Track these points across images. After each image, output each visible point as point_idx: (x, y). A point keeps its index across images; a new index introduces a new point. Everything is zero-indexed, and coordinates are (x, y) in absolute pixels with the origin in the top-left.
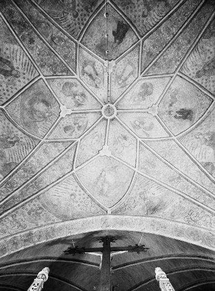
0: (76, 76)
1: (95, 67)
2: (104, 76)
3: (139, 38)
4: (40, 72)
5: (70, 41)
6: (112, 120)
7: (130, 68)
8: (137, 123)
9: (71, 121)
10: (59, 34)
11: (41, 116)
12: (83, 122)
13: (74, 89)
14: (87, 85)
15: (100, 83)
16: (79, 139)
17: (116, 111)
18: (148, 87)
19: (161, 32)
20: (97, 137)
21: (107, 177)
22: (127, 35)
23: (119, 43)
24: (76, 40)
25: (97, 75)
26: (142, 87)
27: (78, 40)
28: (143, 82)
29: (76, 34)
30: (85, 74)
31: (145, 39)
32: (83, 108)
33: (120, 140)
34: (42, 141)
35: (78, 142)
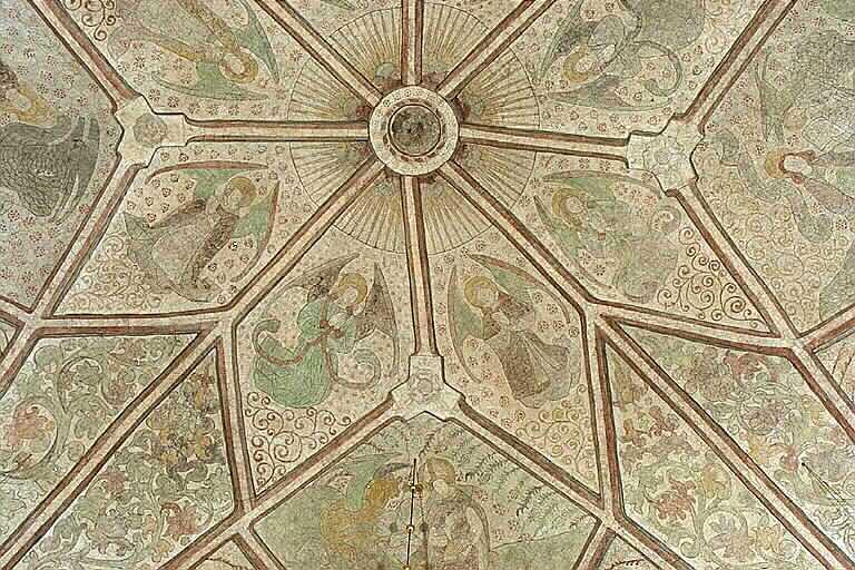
0: (223, 331)
2: (206, 165)
4: (220, 539)
5: (27, 370)
11: (448, 520)
12: (475, 283)
13: (289, 336)
15: (248, 190)
16: (590, 310)
17: (413, 91)
20: (570, 201)
21: (823, 143)
24: (23, 340)
27: (19, 326)
30: (205, 273)
32: (397, 283)
33: (586, 63)
34: (615, 527)
35: (610, 320)
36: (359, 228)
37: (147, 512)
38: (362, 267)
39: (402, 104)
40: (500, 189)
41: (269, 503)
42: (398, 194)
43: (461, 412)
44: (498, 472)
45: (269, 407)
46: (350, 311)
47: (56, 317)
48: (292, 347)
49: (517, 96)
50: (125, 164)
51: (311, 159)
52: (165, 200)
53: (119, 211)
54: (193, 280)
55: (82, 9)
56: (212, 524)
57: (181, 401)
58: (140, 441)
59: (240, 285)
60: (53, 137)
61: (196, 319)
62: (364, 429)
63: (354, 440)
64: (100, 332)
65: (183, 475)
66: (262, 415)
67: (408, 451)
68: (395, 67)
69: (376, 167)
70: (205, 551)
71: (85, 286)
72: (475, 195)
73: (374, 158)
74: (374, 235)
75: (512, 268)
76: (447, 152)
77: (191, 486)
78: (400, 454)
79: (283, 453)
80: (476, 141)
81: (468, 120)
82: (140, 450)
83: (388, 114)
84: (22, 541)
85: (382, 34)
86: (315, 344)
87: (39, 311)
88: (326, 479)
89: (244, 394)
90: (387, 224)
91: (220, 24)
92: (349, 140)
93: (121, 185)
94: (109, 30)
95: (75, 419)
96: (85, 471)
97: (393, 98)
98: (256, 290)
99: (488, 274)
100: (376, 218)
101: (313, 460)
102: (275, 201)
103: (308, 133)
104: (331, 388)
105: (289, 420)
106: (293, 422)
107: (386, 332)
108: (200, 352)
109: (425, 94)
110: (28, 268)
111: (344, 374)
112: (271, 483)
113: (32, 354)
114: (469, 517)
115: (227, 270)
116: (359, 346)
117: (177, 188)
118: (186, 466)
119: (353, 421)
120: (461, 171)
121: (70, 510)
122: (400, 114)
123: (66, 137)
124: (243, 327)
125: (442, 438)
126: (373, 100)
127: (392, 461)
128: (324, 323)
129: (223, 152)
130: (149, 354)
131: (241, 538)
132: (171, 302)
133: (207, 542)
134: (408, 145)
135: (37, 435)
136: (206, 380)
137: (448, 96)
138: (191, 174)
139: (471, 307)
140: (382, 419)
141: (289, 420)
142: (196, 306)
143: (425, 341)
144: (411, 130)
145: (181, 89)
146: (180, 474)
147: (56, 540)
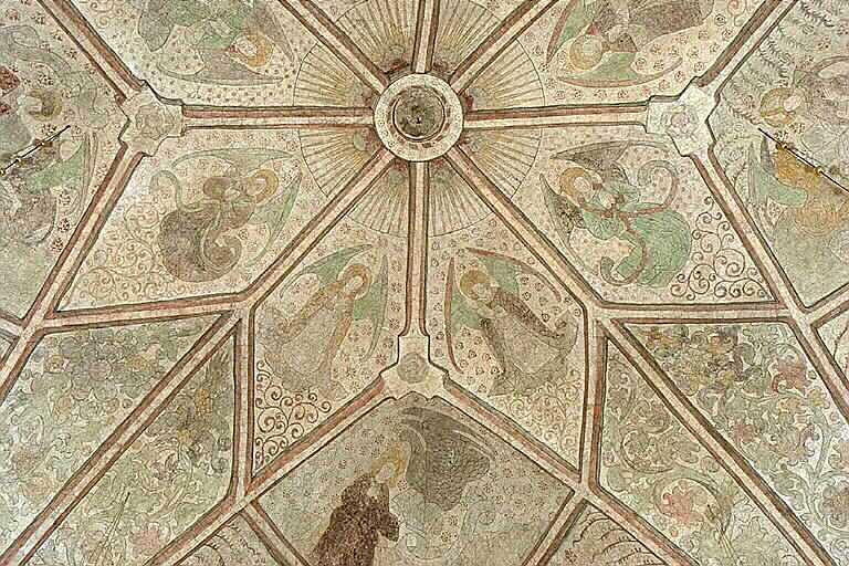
0: (606, 316)
1: (494, 362)
2: (448, 314)
3: (251, 511)
5: (628, 499)
6: (402, 66)
7: (298, 357)
8: (246, 47)
9: (651, 59)
10: (684, 531)
12: (575, 56)
13: (617, 249)
14: (540, 268)
15: (473, 277)
18: (193, 258)
19: (135, 538)
22: (322, 522)
23: (364, 481)
25: (485, 323)
26: (226, 258)
27: (585, 503)
28: (221, 286)
29: (595, 531)
30: (551, 325)
31: (219, 509)
32: (576, 138)
36: (515, 173)
37: (779, 406)
38: (554, 171)
39: (393, 128)
40: (479, 30)
41: (783, 291)
42: (483, 133)
43: (709, 86)
44: (780, 46)
45: (687, 277)
46: (596, 186)
47: (580, 470)
48: (630, 248)
49: (385, 13)
50: (442, 392)
51: (446, 217)
52: (479, 356)
53: (486, 400)
54: (557, 337)
55: (302, 422)
56: (800, 348)
57: (672, 361)
58: (708, 404)
59: (564, 294)
60: (420, 445)
61: (593, 342)
62: (718, 187)
63: (728, 198)
64: (598, 429)
65: (746, 366)
66: (694, 283)
67: (747, 138)
68: (356, 133)
69: (454, 156)
70: (824, 360)
71: (553, 440)
72: (484, 59)
73: (445, 157)
74: (523, 158)
75: (563, 18)
76: (441, 86)
77: (758, 360)
78: (752, 145)
79: (735, 268)
80: (430, 53)
81: (408, 60)
82: (716, 404)
83: (402, 142)
84: (788, 528)
85: (325, 146)
86: (628, 224)
87: (574, 485)
88: (766, 227)
89: (671, 299)
90: (512, 145)
91: (318, 297)
92: (427, 180)
93: (461, 398)
94: (321, 399)
95: (681, 462)
96: (729, 461)
97: (387, 138)
98: (569, 282)
99: (568, 45)
100: (505, 155)
101: (744, 240)
102: (485, 253)
103: (419, 220)
104: (675, 212)
105: (702, 258)
106: (705, 254)
107: (621, 152)
108: (625, 341)
109: (382, 107)
110: (536, 486)
111: (660, 199)
112: (764, 285)
113: (615, 494)
114: (827, 76)
115: (548, 305)
116: (633, 181)
117: (468, 344)
118: (737, 363)
119: (709, 194)
120: (460, 71)
121: (766, 478)
122: (403, 129)
123: (419, 434)
124: (606, 294)
125: (738, 101)
126: (388, 158)
127: (757, 153)
128: (607, 213)
129: (436, 299)
130: (624, 386)
131: (816, 321)
132: (575, 360)
133: (815, 356)
134: (433, 121)
135: (691, 497)
136: (654, 335)
137: (384, 85)
138: (456, 330)
139: (601, 63)
140: (710, 168)
141: (702, 258)
142: (581, 338)
143: (632, 117)
144: (417, 119)
145: (376, 335)
146: (745, 369)
147: (794, 495)
